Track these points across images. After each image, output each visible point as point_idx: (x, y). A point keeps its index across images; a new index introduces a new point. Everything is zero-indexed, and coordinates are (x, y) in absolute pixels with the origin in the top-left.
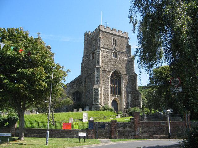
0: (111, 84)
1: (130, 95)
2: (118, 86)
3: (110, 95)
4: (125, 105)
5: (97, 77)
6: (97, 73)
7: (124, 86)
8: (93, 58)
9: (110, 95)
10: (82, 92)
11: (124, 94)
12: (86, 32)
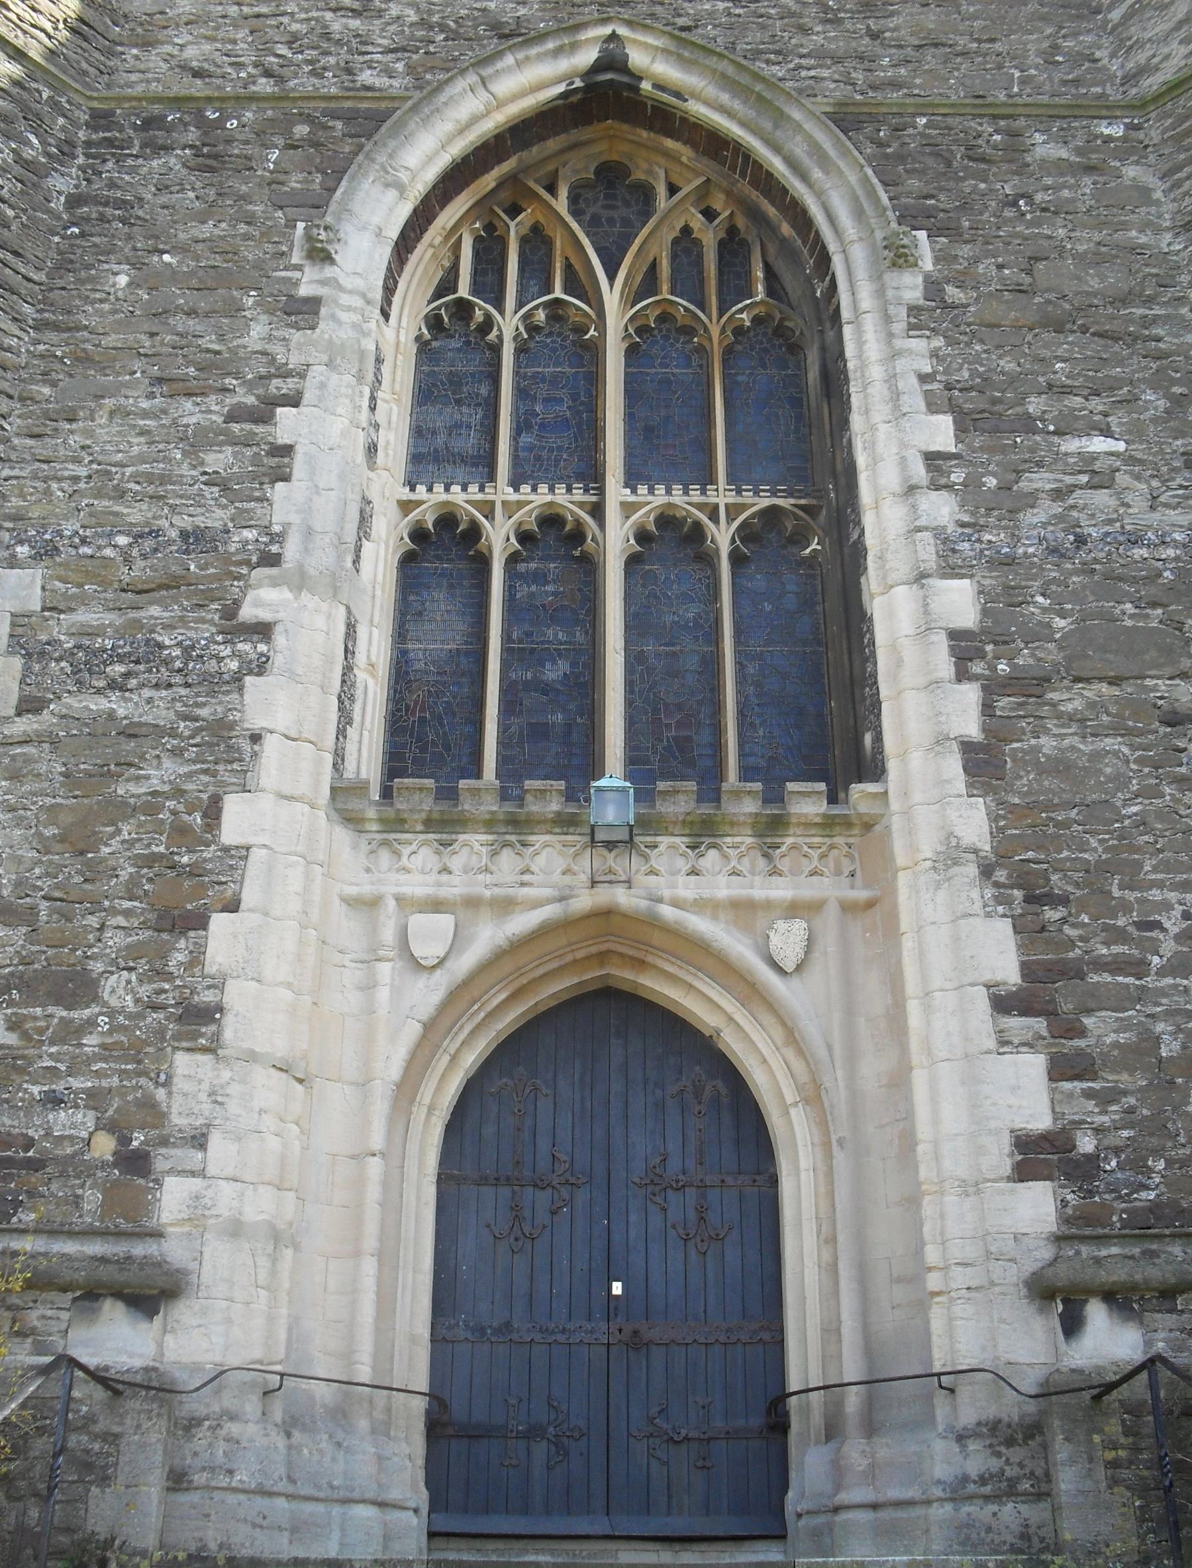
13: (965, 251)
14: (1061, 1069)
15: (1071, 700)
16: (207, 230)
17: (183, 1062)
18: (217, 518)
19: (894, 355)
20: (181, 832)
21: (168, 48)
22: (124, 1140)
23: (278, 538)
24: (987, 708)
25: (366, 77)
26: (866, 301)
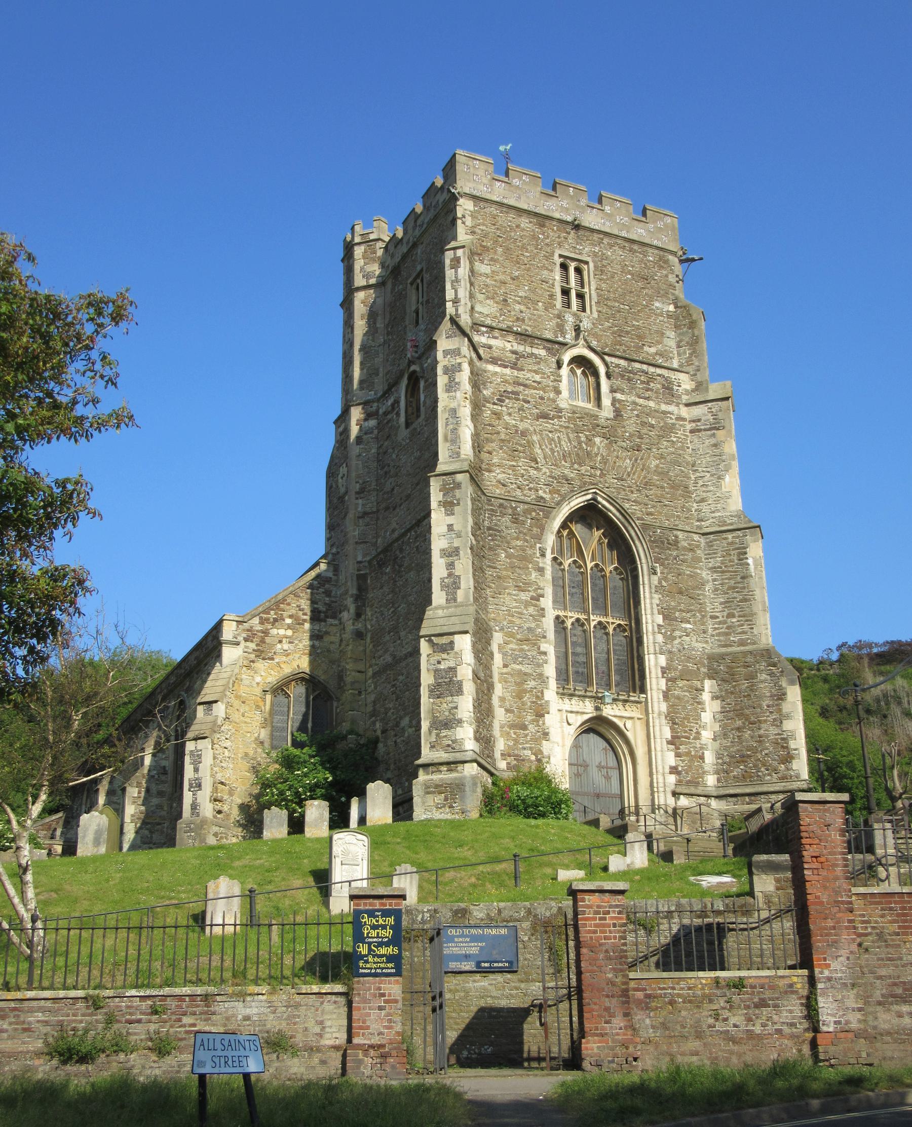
0: (559, 602)
2: (613, 621)
3: (551, 694)
4: (674, 770)
5: (445, 553)
6: (450, 520)
7: (659, 619)
9: (551, 694)
10: (340, 677)
11: (663, 682)
13: (666, 571)
14: (677, 755)
15: (681, 683)
16: (519, 543)
17: (544, 742)
18: (533, 625)
19: (651, 598)
20: (537, 697)
21: (494, 474)
22: (536, 757)
23: (545, 632)
24: (667, 684)
25: (541, 493)
26: (646, 582)
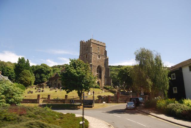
1: (106, 79)
8: (87, 57)
12: (81, 41)
